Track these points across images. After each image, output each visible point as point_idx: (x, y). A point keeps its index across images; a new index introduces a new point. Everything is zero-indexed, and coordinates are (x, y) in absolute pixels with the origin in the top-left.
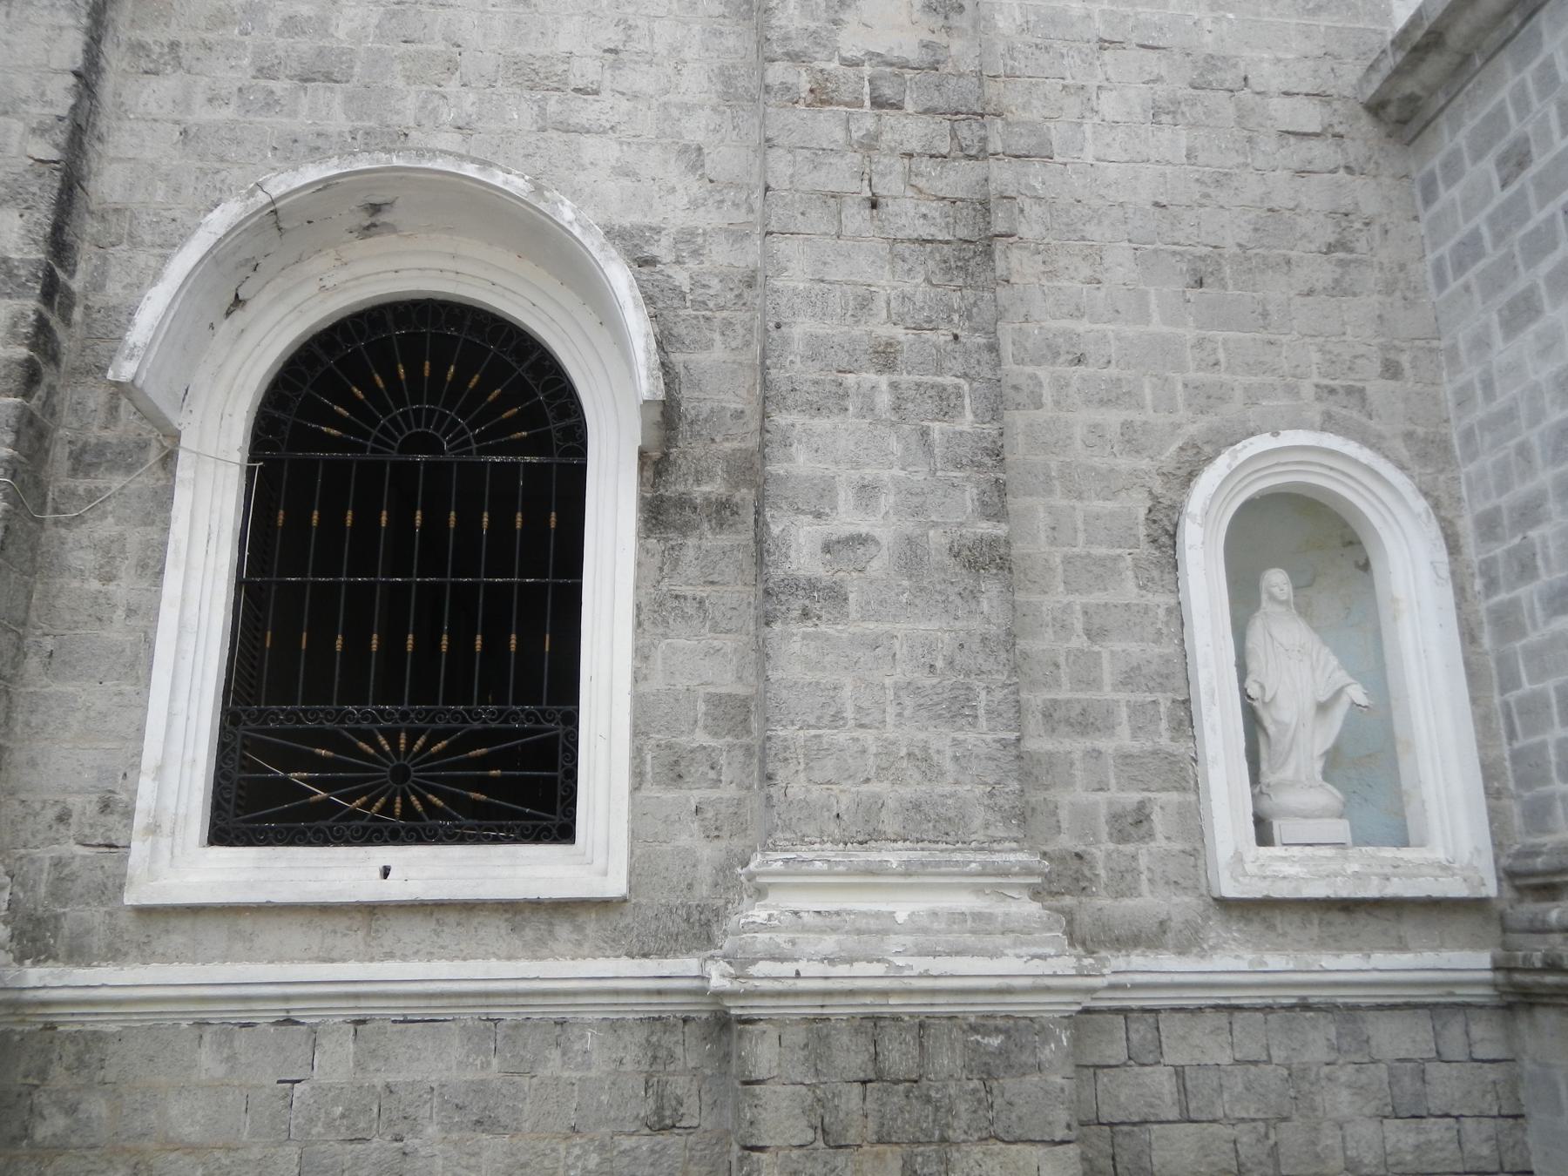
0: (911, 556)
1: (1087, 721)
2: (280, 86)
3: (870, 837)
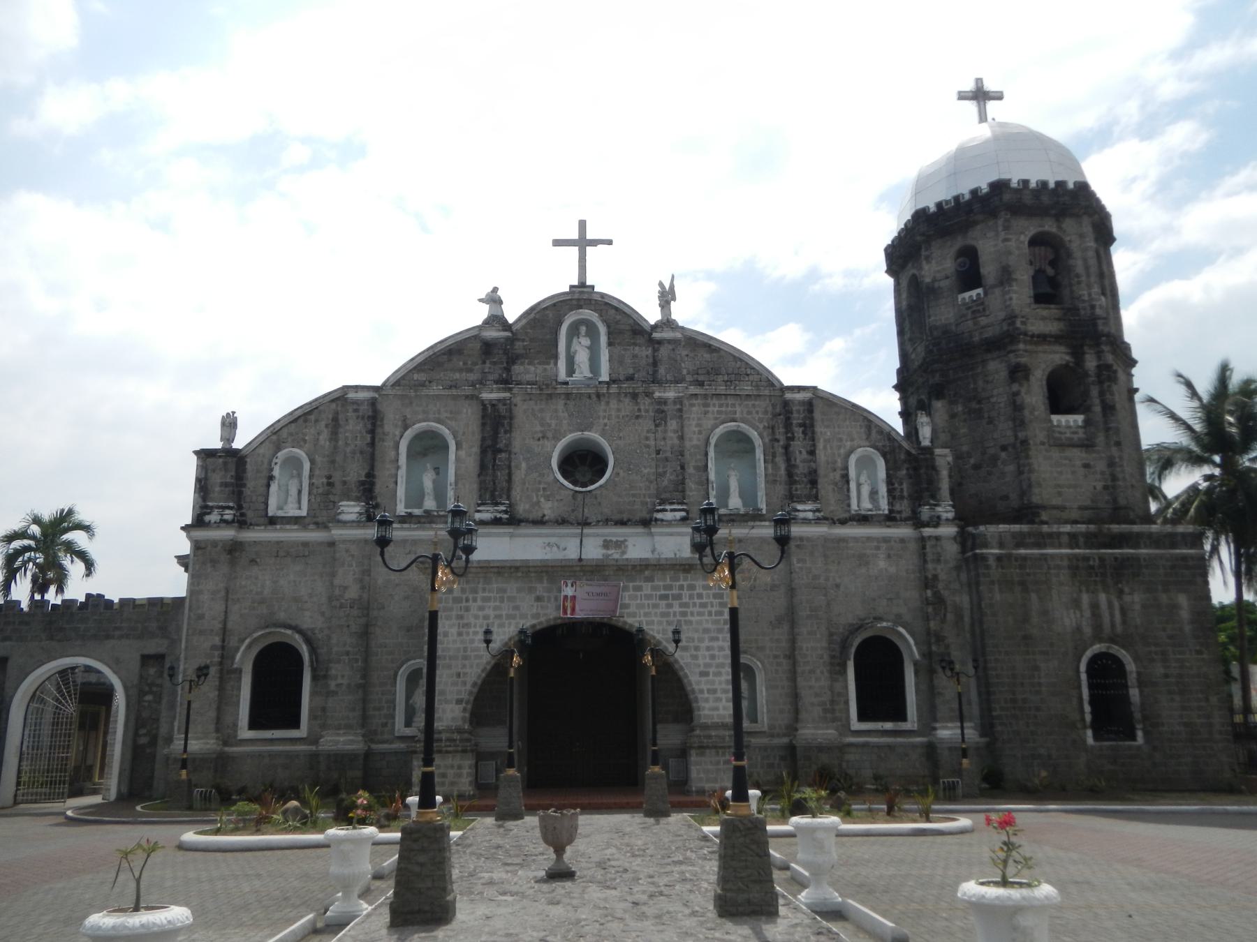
0: (349, 686)
1: (379, 709)
2: (256, 605)
3: (339, 729)
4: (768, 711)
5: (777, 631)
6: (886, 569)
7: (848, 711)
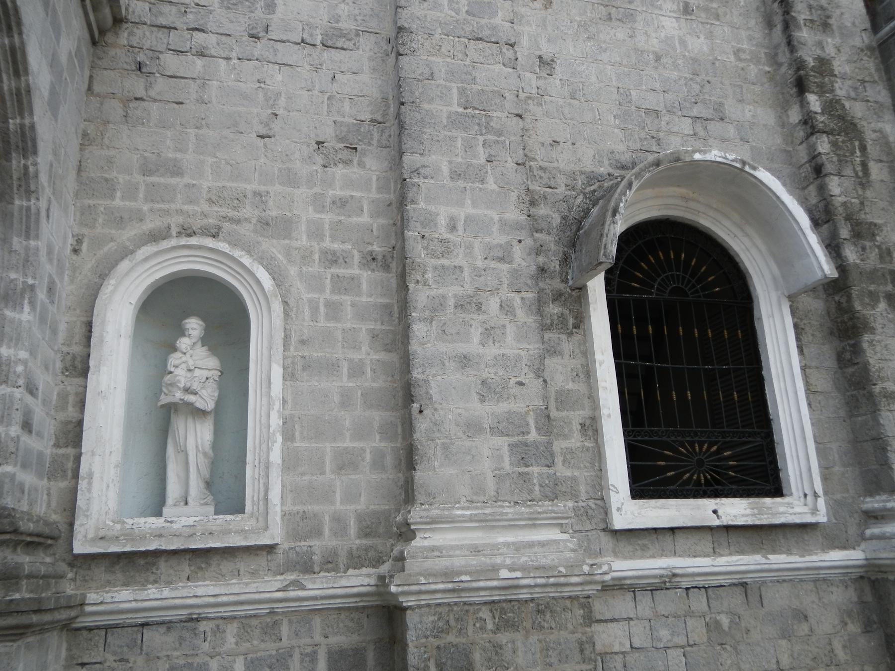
4: (290, 463)
5: (339, 171)
6: (683, 42)
7: (598, 455)
